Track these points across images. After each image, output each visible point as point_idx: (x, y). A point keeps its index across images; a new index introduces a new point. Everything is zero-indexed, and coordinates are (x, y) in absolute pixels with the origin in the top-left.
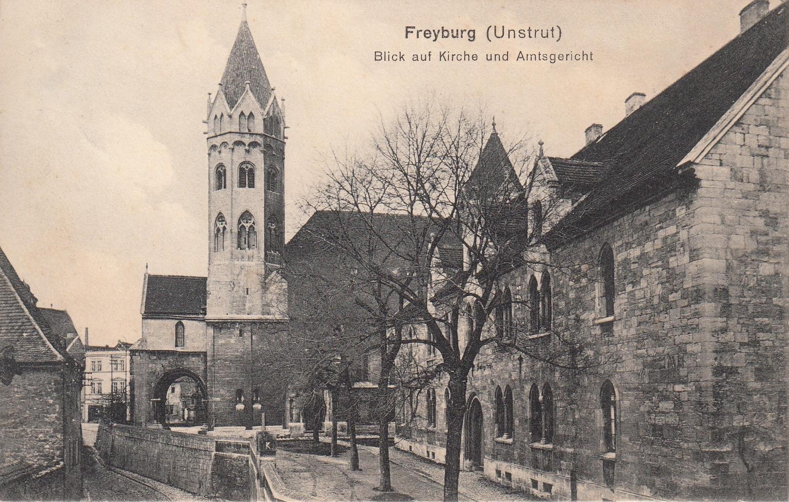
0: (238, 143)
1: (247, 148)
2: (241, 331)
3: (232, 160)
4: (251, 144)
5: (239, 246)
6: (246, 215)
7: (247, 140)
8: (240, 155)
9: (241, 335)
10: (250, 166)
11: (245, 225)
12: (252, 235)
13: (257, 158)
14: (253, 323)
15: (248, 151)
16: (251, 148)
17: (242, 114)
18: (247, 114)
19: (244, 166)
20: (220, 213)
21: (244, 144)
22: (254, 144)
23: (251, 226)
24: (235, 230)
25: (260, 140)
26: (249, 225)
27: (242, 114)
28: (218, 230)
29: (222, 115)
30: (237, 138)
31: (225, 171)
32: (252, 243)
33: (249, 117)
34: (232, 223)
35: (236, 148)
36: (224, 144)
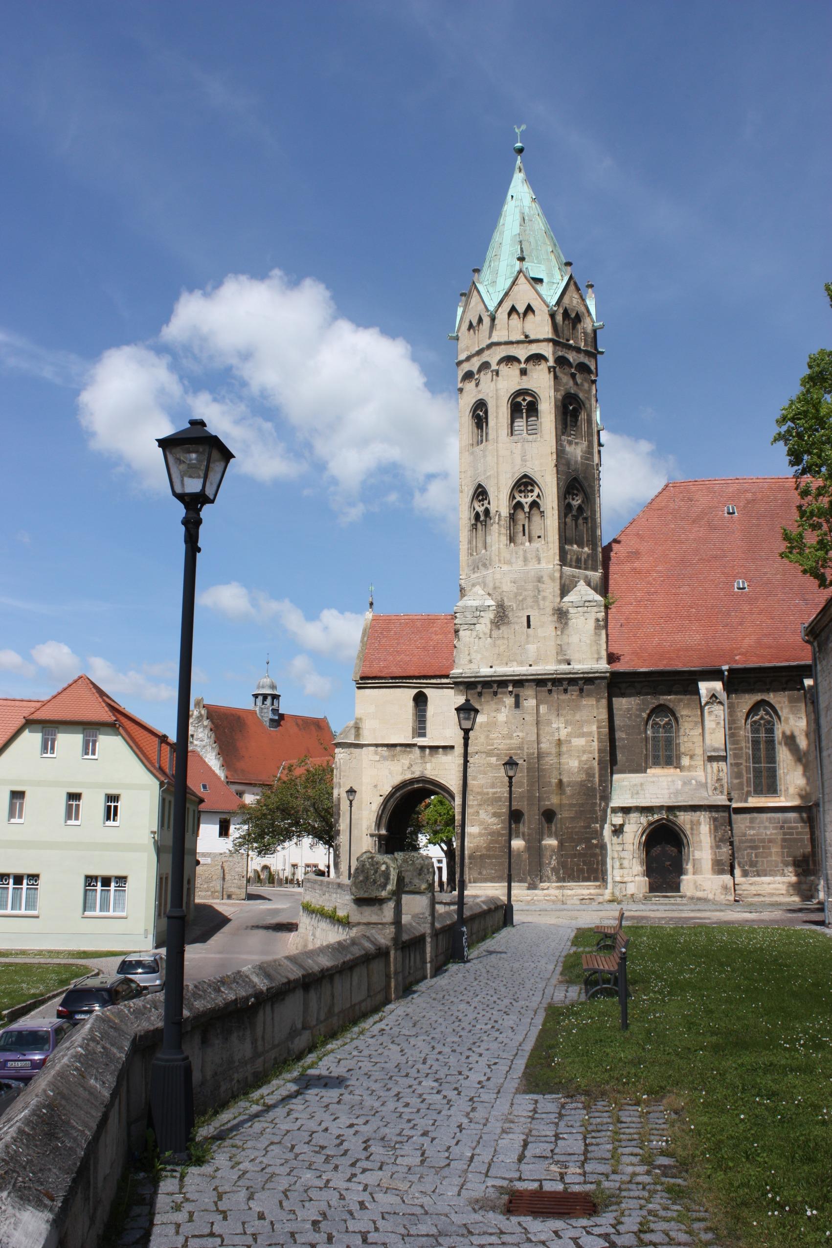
0: (510, 360)
1: (523, 366)
2: (517, 697)
3: (498, 390)
4: (529, 359)
5: (512, 539)
6: (525, 483)
7: (522, 353)
8: (509, 381)
9: (517, 705)
10: (529, 399)
11: (523, 500)
12: (536, 518)
13: (541, 382)
14: (540, 682)
15: (523, 372)
16: (530, 367)
17: (513, 310)
18: (521, 309)
19: (519, 399)
20: (480, 486)
21: (517, 360)
22: (537, 358)
23: (534, 505)
24: (505, 511)
25: (547, 350)
26: (529, 500)
27: (513, 310)
28: (477, 516)
29: (480, 320)
30: (503, 352)
31: (486, 413)
32: (535, 533)
33: (525, 313)
34: (499, 503)
35: (503, 369)
36: (485, 366)
